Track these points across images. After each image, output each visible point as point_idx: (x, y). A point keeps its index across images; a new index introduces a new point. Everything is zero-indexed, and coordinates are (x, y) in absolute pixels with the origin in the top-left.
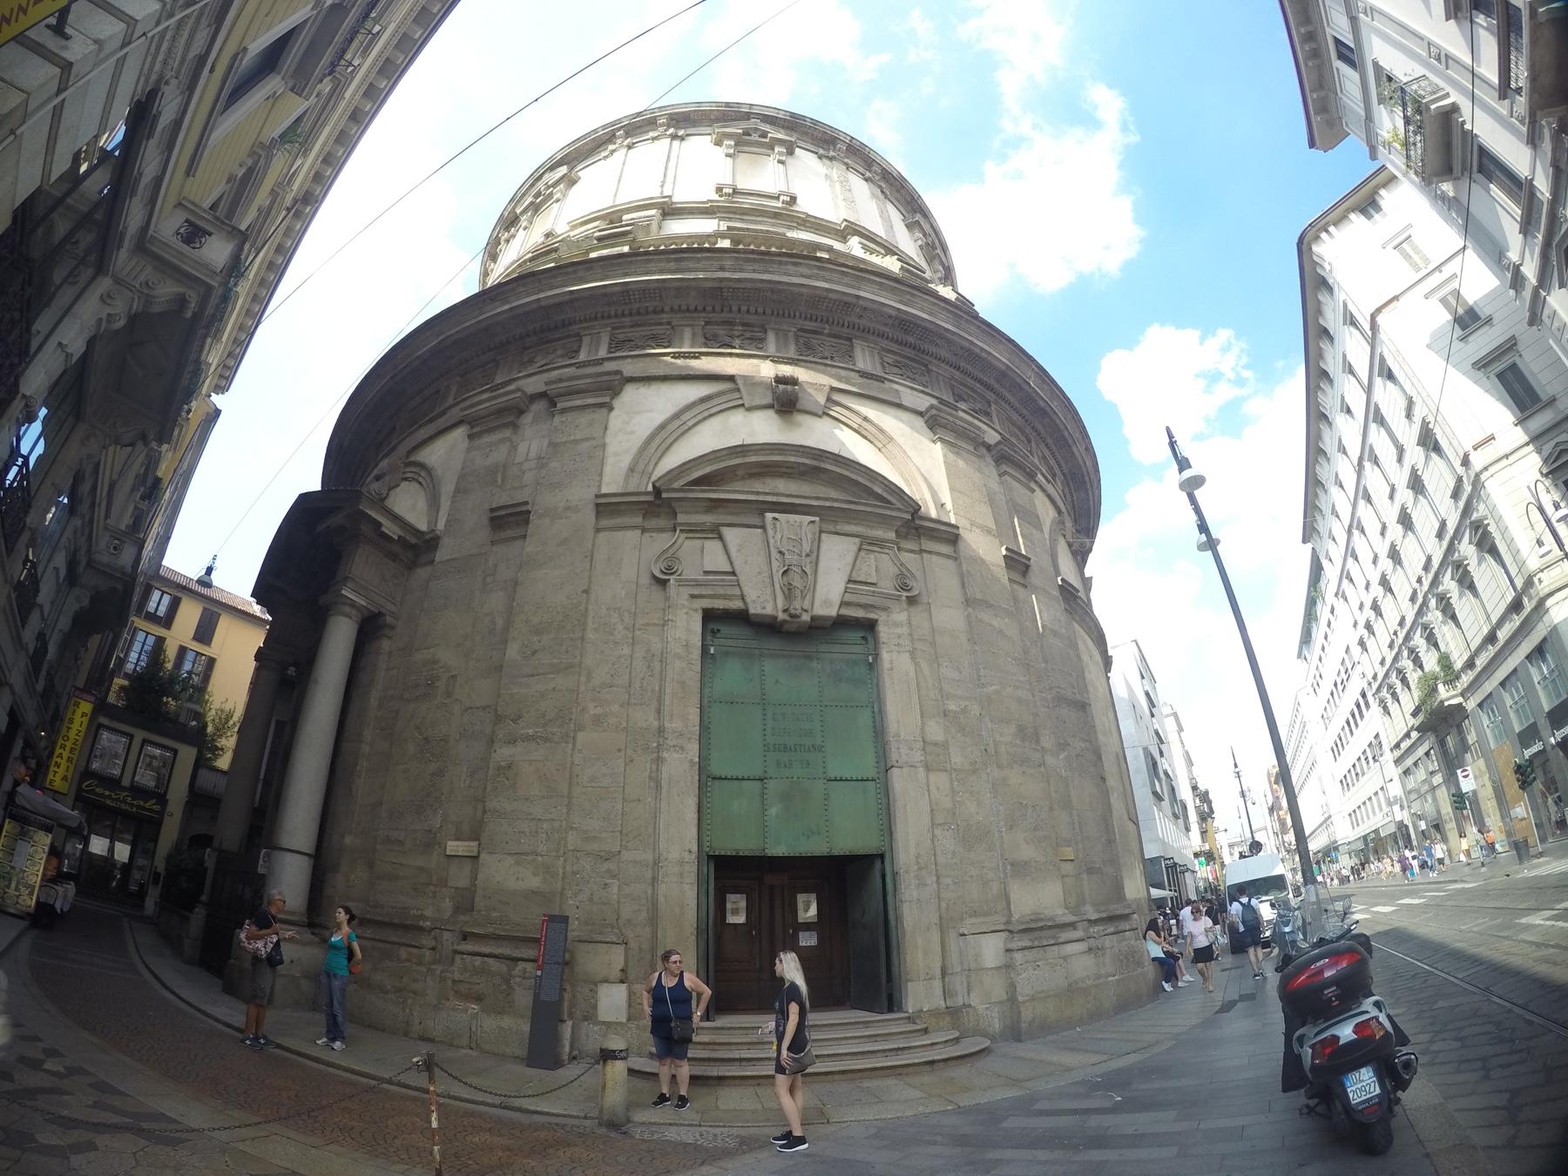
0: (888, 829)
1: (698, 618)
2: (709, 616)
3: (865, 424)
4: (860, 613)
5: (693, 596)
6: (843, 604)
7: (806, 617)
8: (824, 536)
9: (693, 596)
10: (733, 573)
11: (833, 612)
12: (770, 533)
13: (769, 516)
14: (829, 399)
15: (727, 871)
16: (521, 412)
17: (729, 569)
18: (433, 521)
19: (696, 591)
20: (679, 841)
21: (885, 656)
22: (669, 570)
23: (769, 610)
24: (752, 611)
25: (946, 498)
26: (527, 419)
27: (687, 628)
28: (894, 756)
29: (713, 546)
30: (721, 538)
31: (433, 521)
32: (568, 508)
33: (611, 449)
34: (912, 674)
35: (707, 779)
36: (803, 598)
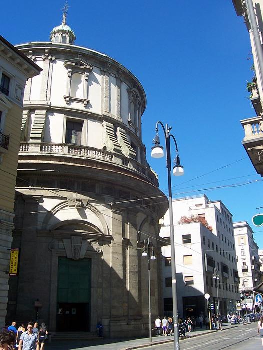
0: (90, 299)
1: (57, 258)
2: (59, 257)
4: (88, 257)
5: (57, 254)
6: (85, 255)
7: (78, 259)
9: (57, 254)
13: (72, 237)
14: (88, 204)
15: (60, 305)
20: (54, 300)
21: (92, 266)
23: (71, 257)
24: (68, 257)
25: (110, 227)
27: (55, 260)
28: (92, 285)
29: (61, 243)
35: (58, 288)
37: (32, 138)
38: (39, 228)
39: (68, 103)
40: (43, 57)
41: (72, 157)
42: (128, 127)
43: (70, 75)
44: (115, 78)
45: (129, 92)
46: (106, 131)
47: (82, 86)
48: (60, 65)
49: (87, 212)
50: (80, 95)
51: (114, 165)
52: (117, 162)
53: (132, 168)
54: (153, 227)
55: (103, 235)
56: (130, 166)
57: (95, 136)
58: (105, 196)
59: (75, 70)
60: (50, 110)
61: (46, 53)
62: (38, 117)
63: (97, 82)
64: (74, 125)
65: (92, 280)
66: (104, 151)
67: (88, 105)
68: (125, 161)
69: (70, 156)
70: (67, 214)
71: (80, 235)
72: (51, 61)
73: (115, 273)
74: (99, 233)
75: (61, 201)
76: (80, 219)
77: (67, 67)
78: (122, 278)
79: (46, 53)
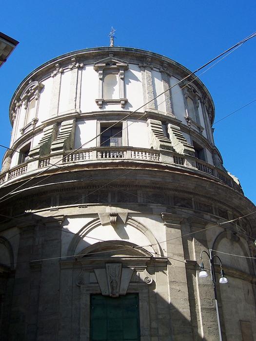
2: (91, 295)
3: (139, 225)
5: (87, 290)
7: (117, 295)
8: (123, 269)
9: (87, 290)
10: (98, 283)
11: (125, 293)
12: (107, 269)
13: (107, 265)
14: (128, 219)
16: (35, 226)
17: (96, 281)
18: (12, 263)
19: (88, 289)
21: (140, 304)
22: (81, 283)
23: (107, 294)
24: (103, 294)
26: (37, 229)
27: (86, 300)
28: (141, 333)
29: (92, 274)
30: (94, 272)
31: (12, 263)
32: (52, 264)
33: (63, 242)
34: (148, 308)
36: (116, 289)
37: (54, 150)
38: (63, 257)
40: (70, 67)
41: (101, 161)
42: (186, 124)
43: (102, 77)
44: (160, 72)
45: (181, 85)
48: (90, 70)
49: (128, 229)
50: (116, 95)
51: (162, 164)
52: (168, 160)
53: (190, 166)
54: (237, 245)
55: (152, 258)
56: (187, 165)
57: (139, 137)
58: (153, 206)
59: (106, 71)
60: (79, 118)
61: (73, 61)
62: (65, 127)
63: (136, 79)
64: (111, 130)
65: (141, 325)
66: (152, 151)
67: (126, 103)
68: (178, 158)
69: (99, 161)
70: (104, 234)
71: (118, 261)
72: (79, 68)
73: (177, 312)
74: (147, 256)
75: (92, 219)
76: (120, 239)
78: (189, 318)
79: (73, 61)
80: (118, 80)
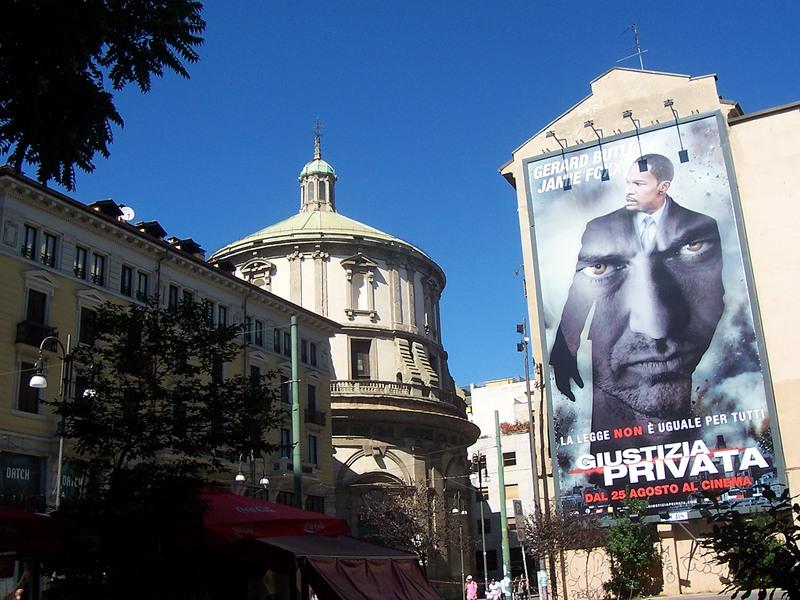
25: (413, 477)
39: (351, 318)
42: (425, 337)
44: (406, 269)
46: (399, 351)
47: (365, 290)
48: (335, 263)
49: (385, 460)
50: (363, 304)
53: (435, 399)
54: (461, 467)
55: (406, 487)
56: (431, 397)
57: (388, 361)
58: (406, 440)
59: (356, 270)
61: (318, 249)
64: (360, 347)
67: (375, 318)
68: (425, 391)
70: (364, 465)
71: (379, 488)
72: (324, 259)
75: (356, 450)
76: (379, 469)
77: (345, 267)
79: (318, 249)
80: (365, 281)
